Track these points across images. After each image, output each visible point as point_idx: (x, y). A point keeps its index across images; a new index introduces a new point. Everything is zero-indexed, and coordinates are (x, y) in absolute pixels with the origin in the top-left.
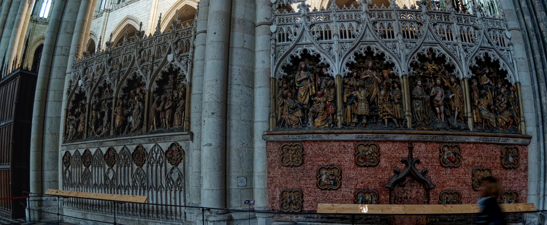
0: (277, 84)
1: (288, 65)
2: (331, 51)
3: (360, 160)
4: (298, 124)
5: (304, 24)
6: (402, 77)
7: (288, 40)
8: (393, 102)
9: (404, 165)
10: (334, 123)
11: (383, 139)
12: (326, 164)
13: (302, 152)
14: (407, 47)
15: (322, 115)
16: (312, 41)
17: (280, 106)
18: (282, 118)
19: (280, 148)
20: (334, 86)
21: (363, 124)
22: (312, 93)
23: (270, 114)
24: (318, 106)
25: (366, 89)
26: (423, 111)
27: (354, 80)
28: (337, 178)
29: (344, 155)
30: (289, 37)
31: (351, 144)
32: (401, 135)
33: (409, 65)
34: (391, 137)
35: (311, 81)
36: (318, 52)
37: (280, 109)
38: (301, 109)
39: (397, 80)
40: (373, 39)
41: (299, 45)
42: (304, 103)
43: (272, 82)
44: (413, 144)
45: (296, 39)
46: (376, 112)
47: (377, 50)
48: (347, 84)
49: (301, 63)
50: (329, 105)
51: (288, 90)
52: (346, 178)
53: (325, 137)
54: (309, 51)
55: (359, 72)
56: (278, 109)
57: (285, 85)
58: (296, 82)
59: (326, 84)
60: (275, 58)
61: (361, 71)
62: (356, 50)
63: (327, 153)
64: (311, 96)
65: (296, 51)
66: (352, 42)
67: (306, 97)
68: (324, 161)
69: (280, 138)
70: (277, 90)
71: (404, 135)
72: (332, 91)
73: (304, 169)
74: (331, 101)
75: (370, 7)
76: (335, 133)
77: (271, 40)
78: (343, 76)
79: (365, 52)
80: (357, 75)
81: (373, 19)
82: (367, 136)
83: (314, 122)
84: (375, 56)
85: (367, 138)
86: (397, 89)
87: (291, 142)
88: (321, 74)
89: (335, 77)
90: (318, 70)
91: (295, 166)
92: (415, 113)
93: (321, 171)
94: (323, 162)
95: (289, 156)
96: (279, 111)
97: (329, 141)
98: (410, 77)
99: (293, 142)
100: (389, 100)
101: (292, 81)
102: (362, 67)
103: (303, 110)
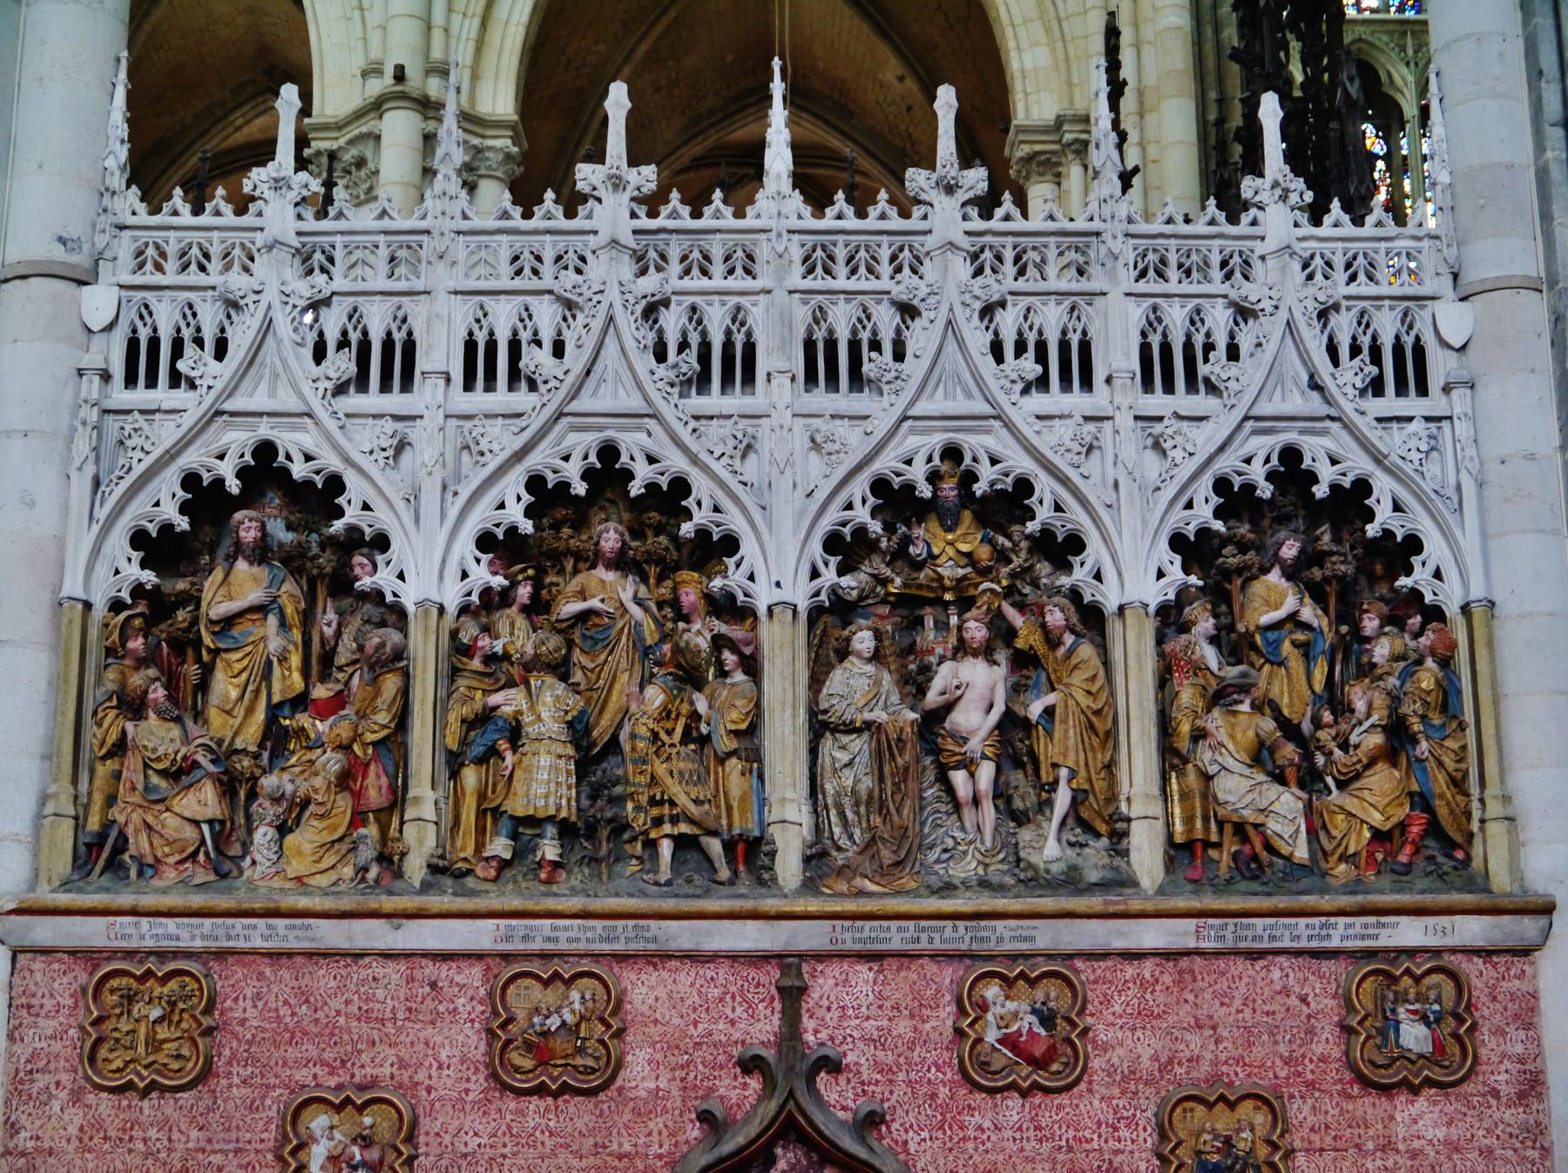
0: (94, 632)
1: (166, 528)
2: (407, 456)
3: (516, 1058)
4: (195, 853)
5: (271, 295)
6: (770, 609)
7: (176, 379)
9: (755, 1083)
11: (641, 946)
12: (333, 1082)
13: (208, 1010)
14: (815, 445)
15: (322, 817)
16: (306, 403)
18: (108, 824)
19: (84, 990)
20: (397, 659)
22: (282, 691)
23: (43, 799)
24: (312, 762)
26: (870, 796)
28: (391, 1155)
29: (430, 1030)
30: (182, 366)
31: (473, 975)
32: (738, 923)
33: (816, 547)
34: (682, 935)
36: (333, 463)
38: (217, 780)
39: (736, 632)
40: (635, 403)
41: (233, 414)
42: (239, 745)
43: (65, 621)
44: (805, 968)
45: (219, 385)
47: (652, 460)
48: (468, 651)
49: (238, 516)
50: (367, 765)
51: (152, 672)
52: (441, 1157)
53: (331, 934)
54: (288, 457)
56: (92, 772)
57: (136, 644)
59: (361, 648)
60: (97, 483)
62: (534, 461)
63: (342, 1020)
64: (281, 704)
65: (215, 447)
66: (519, 415)
67: (250, 711)
68: (324, 1063)
69: (93, 933)
70: (91, 664)
71: (750, 923)
72: (391, 684)
73: (209, 1110)
74: (375, 744)
75: (642, 211)
76: (388, 916)
77: (80, 373)
78: (452, 607)
79: (587, 475)
80: (535, 596)
81: (650, 283)
82: (555, 929)
83: (281, 847)
85: (557, 940)
86: (739, 677)
87: (150, 953)
88: (342, 584)
89: (411, 608)
90: (327, 561)
91: (164, 1089)
92: (826, 807)
93: (305, 1114)
94: (318, 1070)
95: (133, 1031)
96: (98, 783)
97: (359, 956)
98: (816, 613)
99: (162, 955)
100: (686, 738)
101: (182, 615)
102: (568, 552)
103: (228, 786)
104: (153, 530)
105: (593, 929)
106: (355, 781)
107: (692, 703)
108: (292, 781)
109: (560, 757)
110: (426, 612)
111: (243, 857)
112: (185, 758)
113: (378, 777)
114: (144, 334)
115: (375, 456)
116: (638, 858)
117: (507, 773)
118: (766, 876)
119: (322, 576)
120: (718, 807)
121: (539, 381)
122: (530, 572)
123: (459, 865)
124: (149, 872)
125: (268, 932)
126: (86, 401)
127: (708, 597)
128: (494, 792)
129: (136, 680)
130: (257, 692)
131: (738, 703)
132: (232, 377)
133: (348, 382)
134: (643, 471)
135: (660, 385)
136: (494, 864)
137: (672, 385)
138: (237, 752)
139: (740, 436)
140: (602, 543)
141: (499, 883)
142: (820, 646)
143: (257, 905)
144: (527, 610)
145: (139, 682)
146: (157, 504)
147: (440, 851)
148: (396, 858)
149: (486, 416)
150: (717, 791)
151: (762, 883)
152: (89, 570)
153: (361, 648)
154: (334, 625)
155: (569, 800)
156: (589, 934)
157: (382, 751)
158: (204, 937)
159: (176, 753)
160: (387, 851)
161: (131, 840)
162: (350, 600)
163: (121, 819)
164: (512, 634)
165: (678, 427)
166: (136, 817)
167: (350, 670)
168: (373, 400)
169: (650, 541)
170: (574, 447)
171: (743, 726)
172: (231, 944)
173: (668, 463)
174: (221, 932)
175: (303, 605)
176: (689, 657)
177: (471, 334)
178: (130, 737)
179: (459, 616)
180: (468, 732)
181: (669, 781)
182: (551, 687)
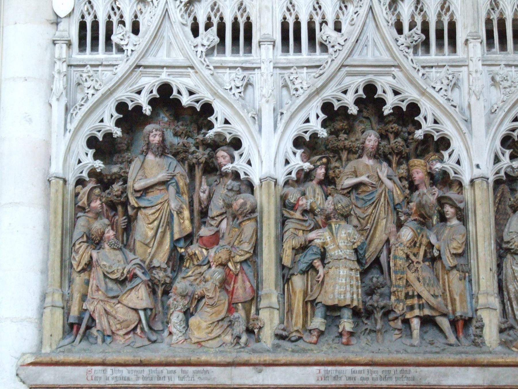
0: (69, 197)
1: (108, 135)
6: (472, 182)
8: (438, 265)
10: (250, 331)
16: (188, 59)
17: (80, 272)
18: (83, 311)
21: (341, 335)
22: (180, 232)
24: (201, 274)
25: (355, 222)
27: (318, 190)
32: (463, 369)
33: (498, 143)
35: (178, 192)
36: (208, 97)
37: (78, 280)
40: (385, 58)
41: (146, 67)
43: (53, 190)
47: (396, 93)
48: (293, 207)
49: (149, 127)
50: (237, 275)
54: (179, 92)
55: (334, 164)
58: (130, 192)
59: (229, 206)
60: (67, 109)
61: (340, 159)
65: (136, 87)
71: (471, 368)
72: (249, 227)
74: (241, 262)
76: (254, 365)
77: (54, 43)
78: (281, 181)
79: (358, 102)
82: (354, 372)
83: (187, 325)
86: (455, 222)
89: (256, 182)
92: (510, 299)
102: (345, 148)
104: (100, 136)
105: (376, 372)
106: (229, 284)
107: (428, 238)
108: (191, 285)
109: (351, 270)
110: (269, 184)
111: (163, 331)
112: (129, 272)
113: (244, 282)
114: (89, 20)
115: (233, 91)
116: (399, 330)
117: (321, 279)
118: (479, 341)
119: (199, 163)
120: (445, 299)
121: (329, 46)
122: (324, 160)
124: (109, 340)
125: (183, 375)
126: (59, 59)
127: (431, 175)
128: (311, 291)
129: (98, 225)
130: (164, 233)
132: (146, 46)
133: (213, 48)
134: (391, 101)
135: (402, 47)
136: (315, 333)
137: (409, 48)
138: (154, 268)
139: (450, 77)
140: (367, 142)
141: (318, 345)
142: (499, 204)
143: (177, 359)
144: (321, 183)
145: (99, 227)
146: (102, 121)
147: (282, 326)
148: (256, 331)
149: (298, 67)
150: (445, 290)
151: (475, 344)
152: (65, 160)
153: (229, 206)
154: (207, 192)
155: (358, 295)
156: (374, 376)
157: (245, 267)
158: (144, 378)
159: (124, 269)
160: (250, 327)
161: (97, 321)
162: (215, 178)
163: (91, 308)
164: (314, 197)
165: (414, 73)
166: (100, 307)
167: (219, 219)
168: (229, 58)
169: (392, 141)
170: (349, 86)
171: (460, 251)
172: (160, 382)
173: (407, 94)
174: (155, 375)
175: (188, 181)
176: (427, 210)
177: (285, 18)
178: (94, 260)
179: (284, 186)
180: (295, 255)
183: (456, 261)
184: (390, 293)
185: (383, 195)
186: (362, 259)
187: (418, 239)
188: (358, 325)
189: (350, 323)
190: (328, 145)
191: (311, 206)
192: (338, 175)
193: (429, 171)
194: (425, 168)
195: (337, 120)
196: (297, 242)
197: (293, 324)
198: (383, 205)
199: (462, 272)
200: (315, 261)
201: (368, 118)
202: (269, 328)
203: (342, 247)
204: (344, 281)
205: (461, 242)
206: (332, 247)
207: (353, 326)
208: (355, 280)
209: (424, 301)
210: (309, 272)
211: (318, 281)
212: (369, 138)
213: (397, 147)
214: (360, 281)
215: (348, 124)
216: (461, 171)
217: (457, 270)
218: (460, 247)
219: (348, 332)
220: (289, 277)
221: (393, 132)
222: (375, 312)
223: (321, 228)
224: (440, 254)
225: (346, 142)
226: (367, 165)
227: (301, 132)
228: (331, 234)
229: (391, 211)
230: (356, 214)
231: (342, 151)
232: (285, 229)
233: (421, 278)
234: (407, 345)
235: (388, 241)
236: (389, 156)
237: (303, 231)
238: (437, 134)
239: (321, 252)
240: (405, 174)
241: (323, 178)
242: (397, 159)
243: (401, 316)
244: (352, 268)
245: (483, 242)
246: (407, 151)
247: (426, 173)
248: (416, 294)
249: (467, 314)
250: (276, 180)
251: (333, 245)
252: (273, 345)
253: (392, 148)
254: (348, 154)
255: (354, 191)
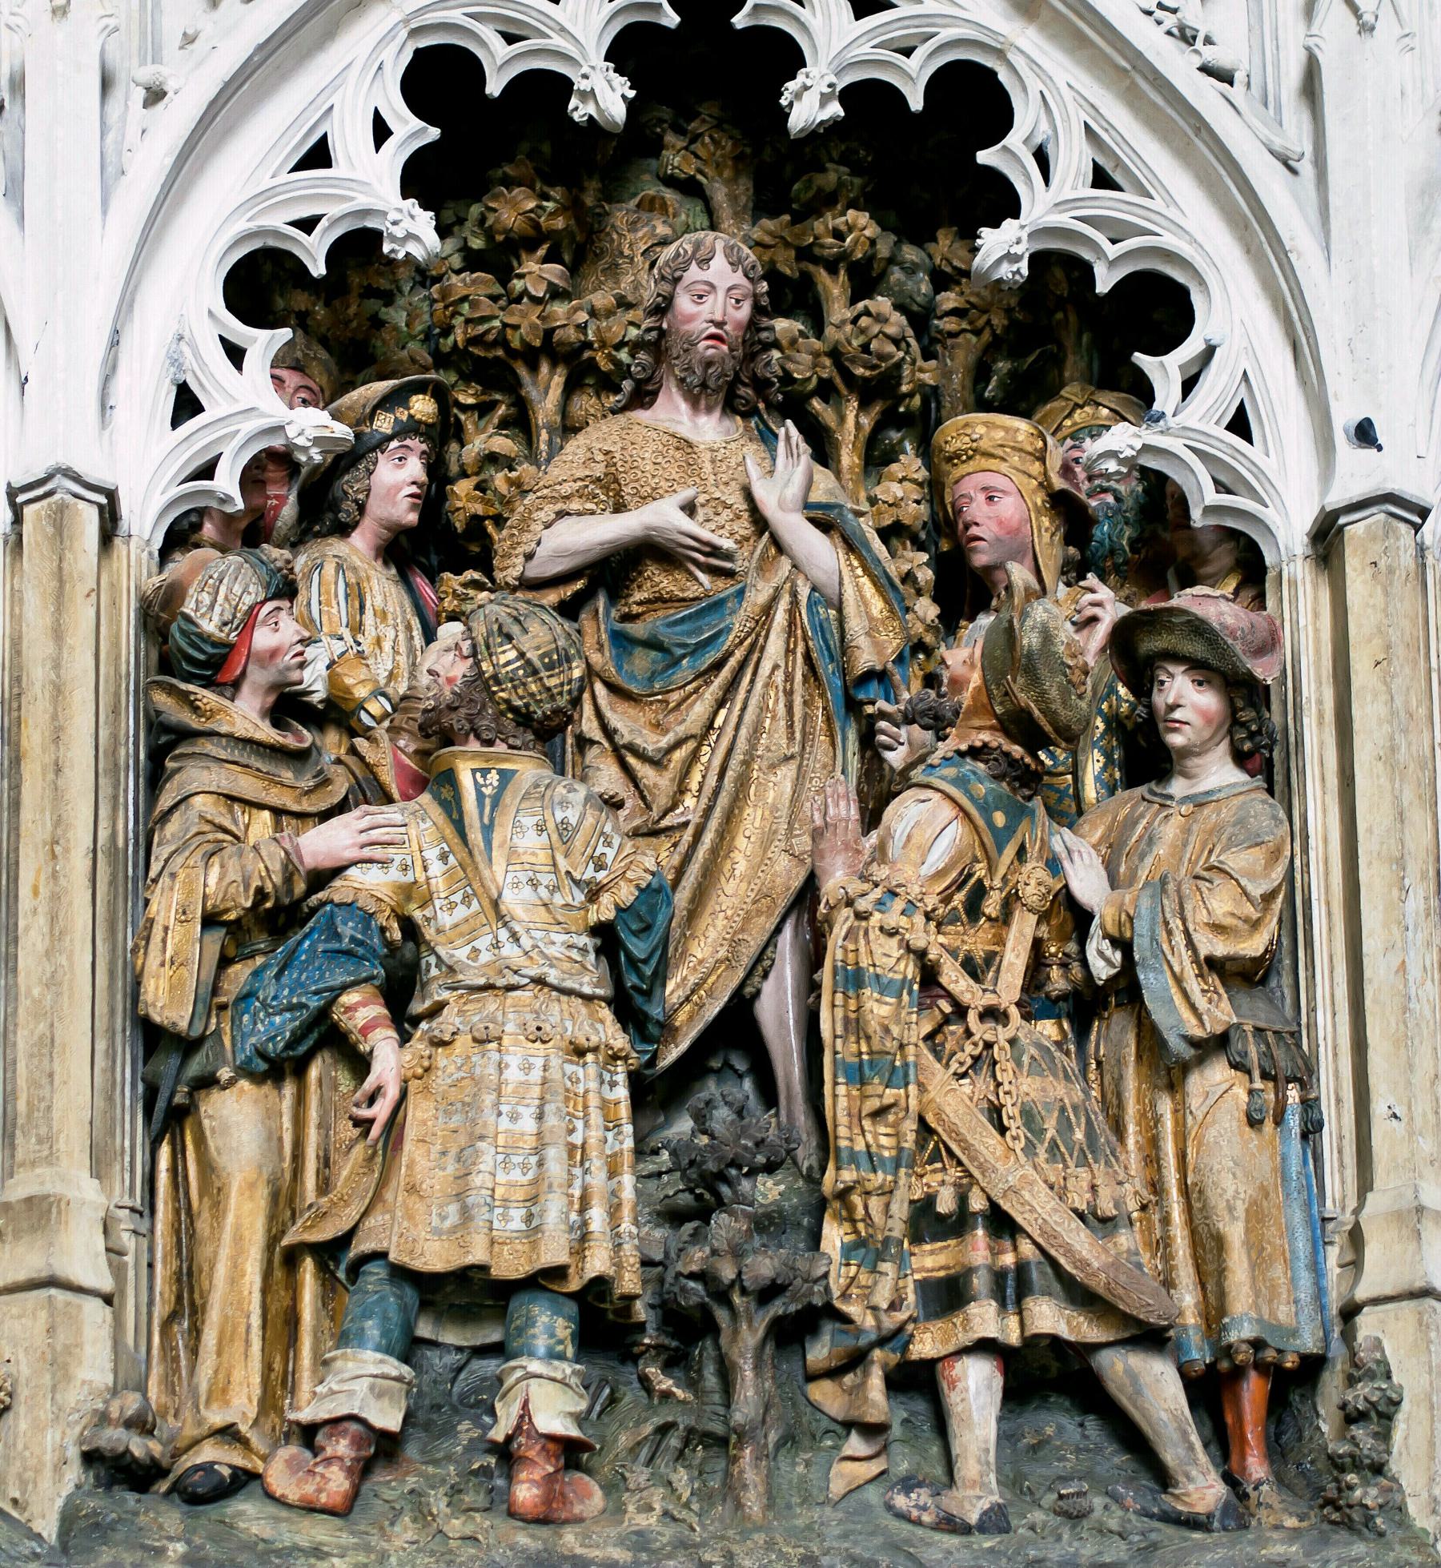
21: (506, 1455)
25: (608, 777)
46: (768, 1224)
84: (822, 135)
107: (1054, 865)
110: (60, 520)
116: (873, 1431)
117: (381, 1110)
118: (1367, 1494)
120: (1162, 1245)
122: (422, 406)
123: (208, 1453)
128: (324, 1186)
131: (1237, 860)
136: (342, 1447)
140: (684, 303)
147: (131, 1403)
150: (1156, 1187)
164: (357, 628)
169: (838, 311)
171: (1253, 946)
180: (225, 962)
181: (987, 1142)
182: (538, 794)
183: (1225, 1004)
184: (820, 1207)
185: (780, 617)
186: (648, 994)
187: (991, 869)
188: (613, 1400)
189: (562, 1382)
190: (447, 330)
191: (333, 679)
192: (507, 503)
193: (1059, 483)
194: (1036, 468)
195: (509, 183)
196: (233, 874)
197: (203, 1387)
198: (779, 677)
199: (1265, 1076)
200: (350, 998)
201: (690, 188)
202: (46, 1411)
203: (519, 912)
204: (528, 1124)
205: (1257, 890)
206: (461, 912)
207: (583, 1405)
208: (596, 1117)
209: (1026, 1248)
210: (314, 1072)
211: (364, 1125)
212: (694, 273)
213: (865, 348)
214: (628, 1129)
215: (573, 207)
216: (1259, 472)
217: (1235, 1066)
218: (1255, 925)
219: (552, 1438)
220: (178, 1099)
221: (844, 256)
222: (721, 1315)
223: (389, 800)
224: (1129, 964)
225: (559, 309)
226: (686, 445)
227: (278, 220)
228: (449, 831)
229: (828, 720)
230: (609, 732)
231: (534, 368)
232: (165, 801)
233: (1010, 1110)
234: (918, 1523)
235: (807, 894)
236: (816, 404)
237: (278, 812)
238: (1113, 251)
239: (389, 944)
240: (915, 512)
241: (412, 518)
242: (866, 422)
243: (882, 1342)
244: (582, 1041)
245: (1395, 892)
246: (928, 378)
247: (1039, 499)
248: (977, 1203)
249: (1294, 1333)
250: (111, 495)
251: (466, 900)
252: (68, 1519)
253: (835, 354)
254: (571, 388)
255: (601, 602)
